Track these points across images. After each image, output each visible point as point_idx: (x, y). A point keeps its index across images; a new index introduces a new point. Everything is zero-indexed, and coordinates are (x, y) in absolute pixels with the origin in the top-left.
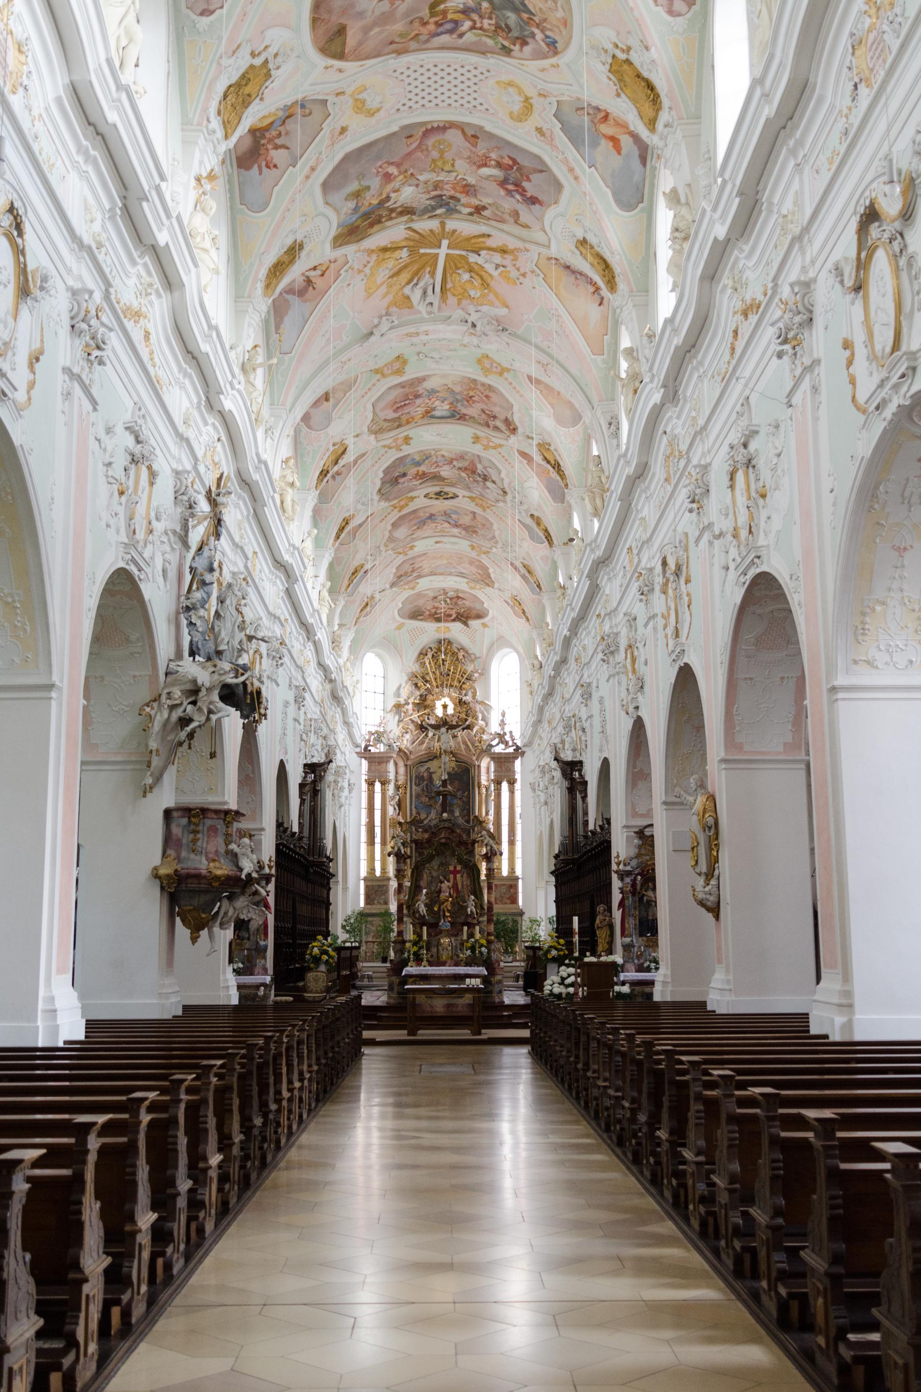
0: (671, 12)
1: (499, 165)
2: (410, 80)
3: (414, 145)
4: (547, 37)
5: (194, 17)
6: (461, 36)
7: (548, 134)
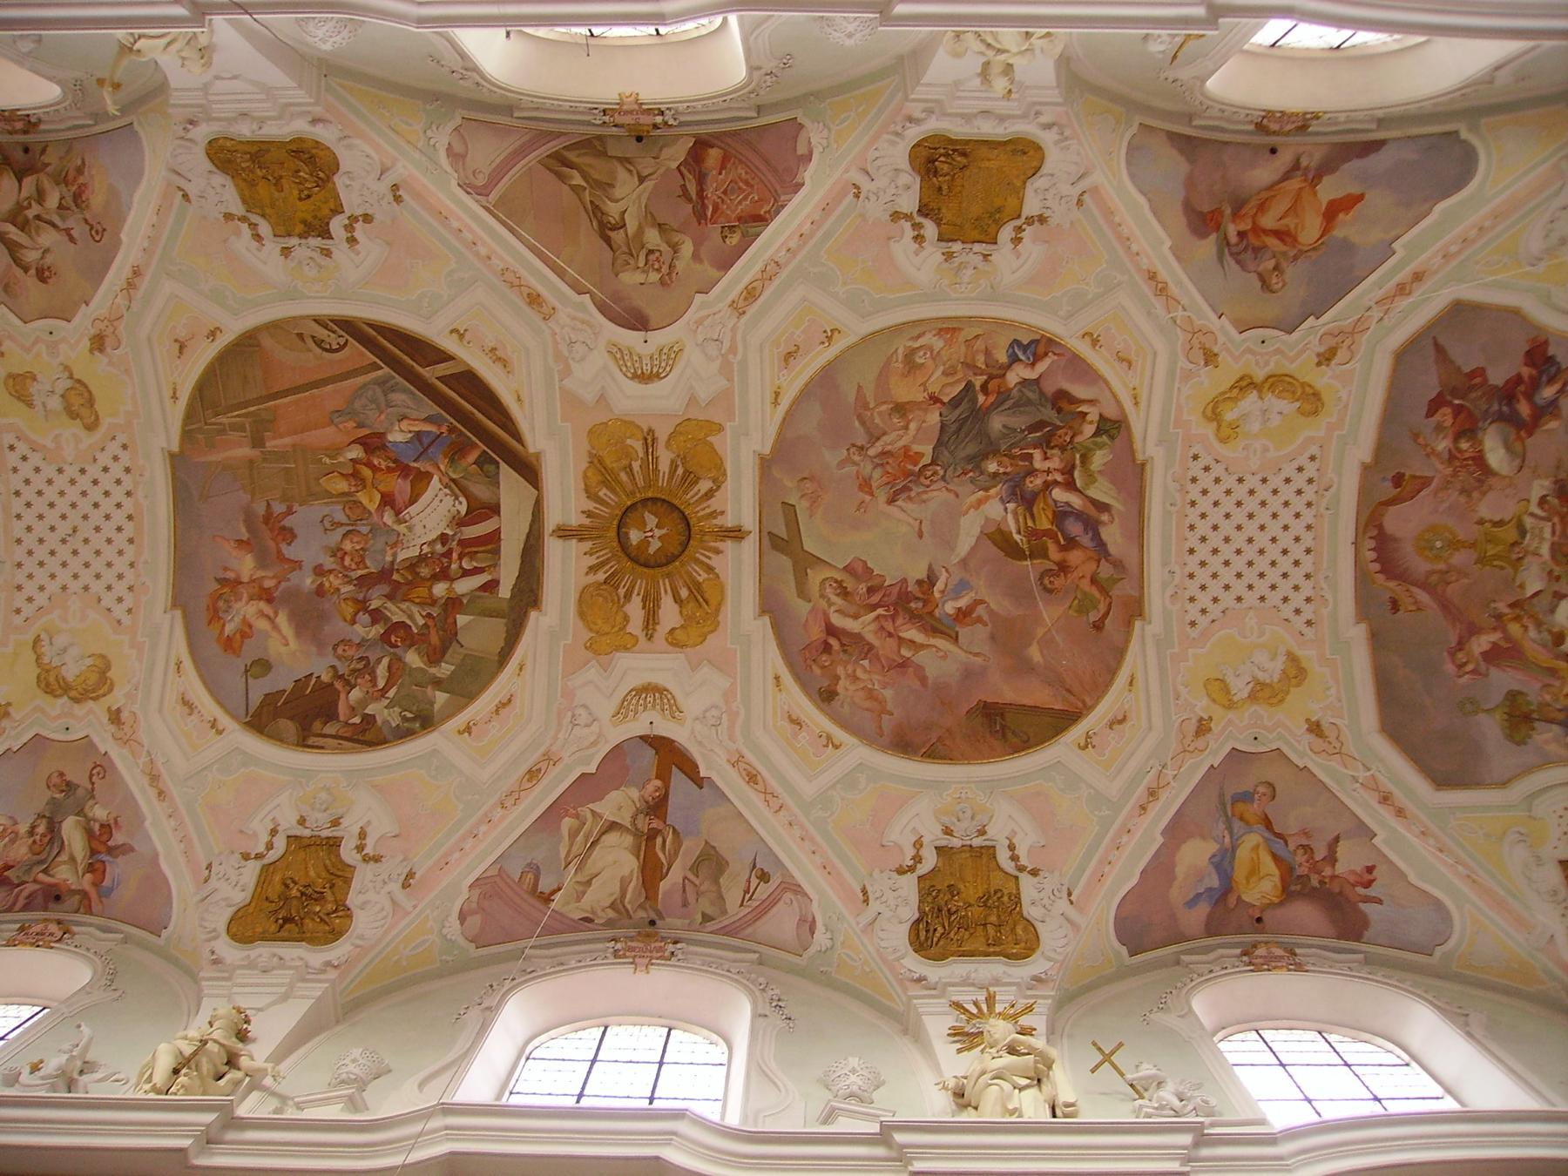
0: (808, 157)
1: (1468, 428)
2: (1227, 599)
3: (1423, 597)
4: (1014, 359)
5: (812, 950)
6: (1103, 507)
7: (1332, 342)
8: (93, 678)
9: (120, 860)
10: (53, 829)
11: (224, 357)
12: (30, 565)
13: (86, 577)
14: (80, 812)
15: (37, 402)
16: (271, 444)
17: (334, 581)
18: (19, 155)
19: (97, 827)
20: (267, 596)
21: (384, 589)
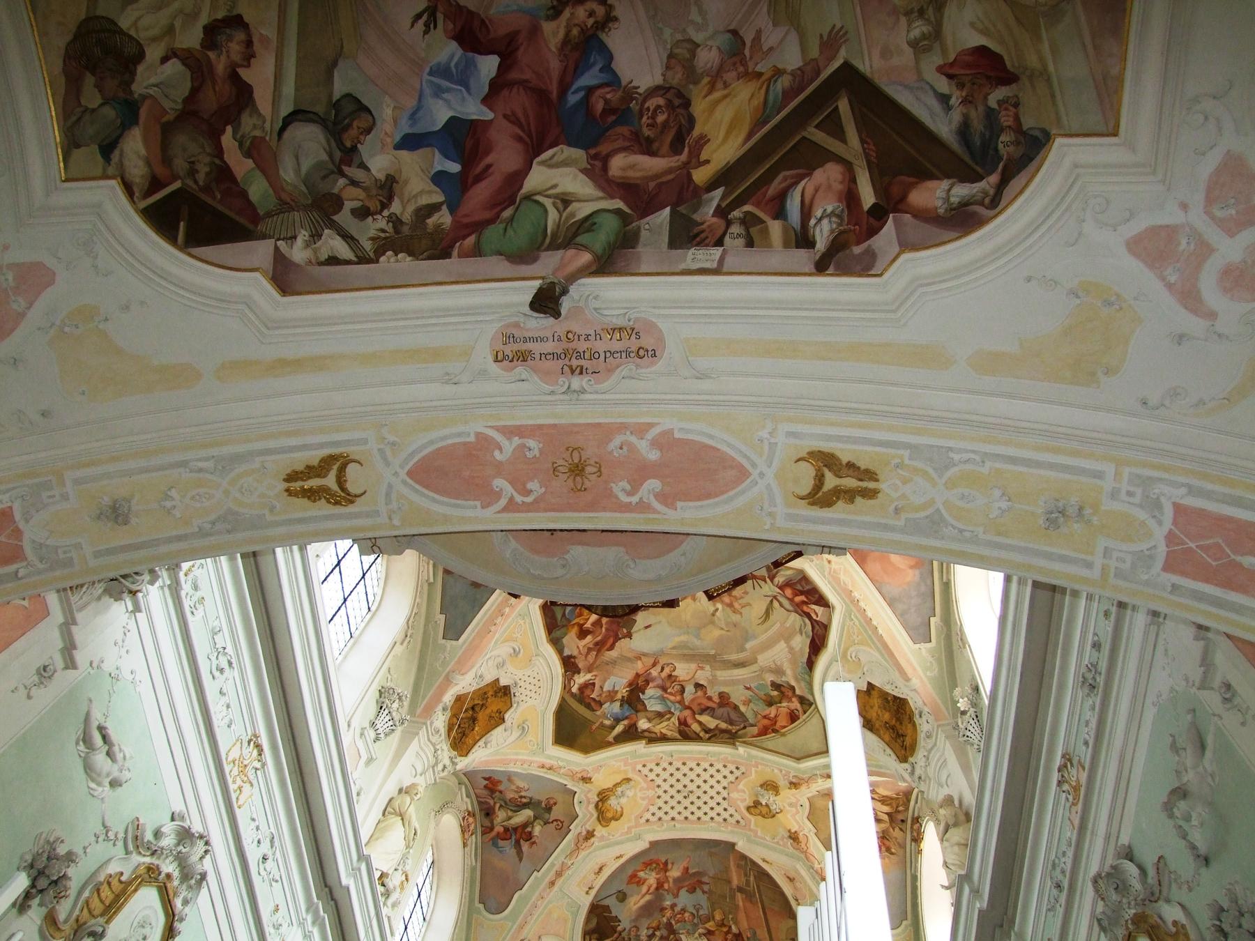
8: (609, 815)
9: (513, 852)
10: (525, 806)
11: (783, 894)
12: (671, 769)
13: (666, 797)
14: (536, 818)
15: (763, 791)
16: (739, 895)
17: (668, 913)
18: (900, 817)
19: (529, 829)
20: (660, 886)
21: (664, 932)
